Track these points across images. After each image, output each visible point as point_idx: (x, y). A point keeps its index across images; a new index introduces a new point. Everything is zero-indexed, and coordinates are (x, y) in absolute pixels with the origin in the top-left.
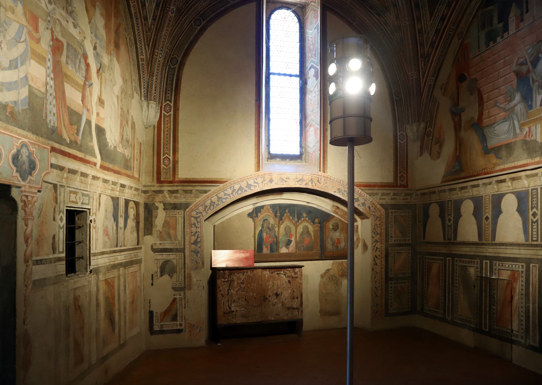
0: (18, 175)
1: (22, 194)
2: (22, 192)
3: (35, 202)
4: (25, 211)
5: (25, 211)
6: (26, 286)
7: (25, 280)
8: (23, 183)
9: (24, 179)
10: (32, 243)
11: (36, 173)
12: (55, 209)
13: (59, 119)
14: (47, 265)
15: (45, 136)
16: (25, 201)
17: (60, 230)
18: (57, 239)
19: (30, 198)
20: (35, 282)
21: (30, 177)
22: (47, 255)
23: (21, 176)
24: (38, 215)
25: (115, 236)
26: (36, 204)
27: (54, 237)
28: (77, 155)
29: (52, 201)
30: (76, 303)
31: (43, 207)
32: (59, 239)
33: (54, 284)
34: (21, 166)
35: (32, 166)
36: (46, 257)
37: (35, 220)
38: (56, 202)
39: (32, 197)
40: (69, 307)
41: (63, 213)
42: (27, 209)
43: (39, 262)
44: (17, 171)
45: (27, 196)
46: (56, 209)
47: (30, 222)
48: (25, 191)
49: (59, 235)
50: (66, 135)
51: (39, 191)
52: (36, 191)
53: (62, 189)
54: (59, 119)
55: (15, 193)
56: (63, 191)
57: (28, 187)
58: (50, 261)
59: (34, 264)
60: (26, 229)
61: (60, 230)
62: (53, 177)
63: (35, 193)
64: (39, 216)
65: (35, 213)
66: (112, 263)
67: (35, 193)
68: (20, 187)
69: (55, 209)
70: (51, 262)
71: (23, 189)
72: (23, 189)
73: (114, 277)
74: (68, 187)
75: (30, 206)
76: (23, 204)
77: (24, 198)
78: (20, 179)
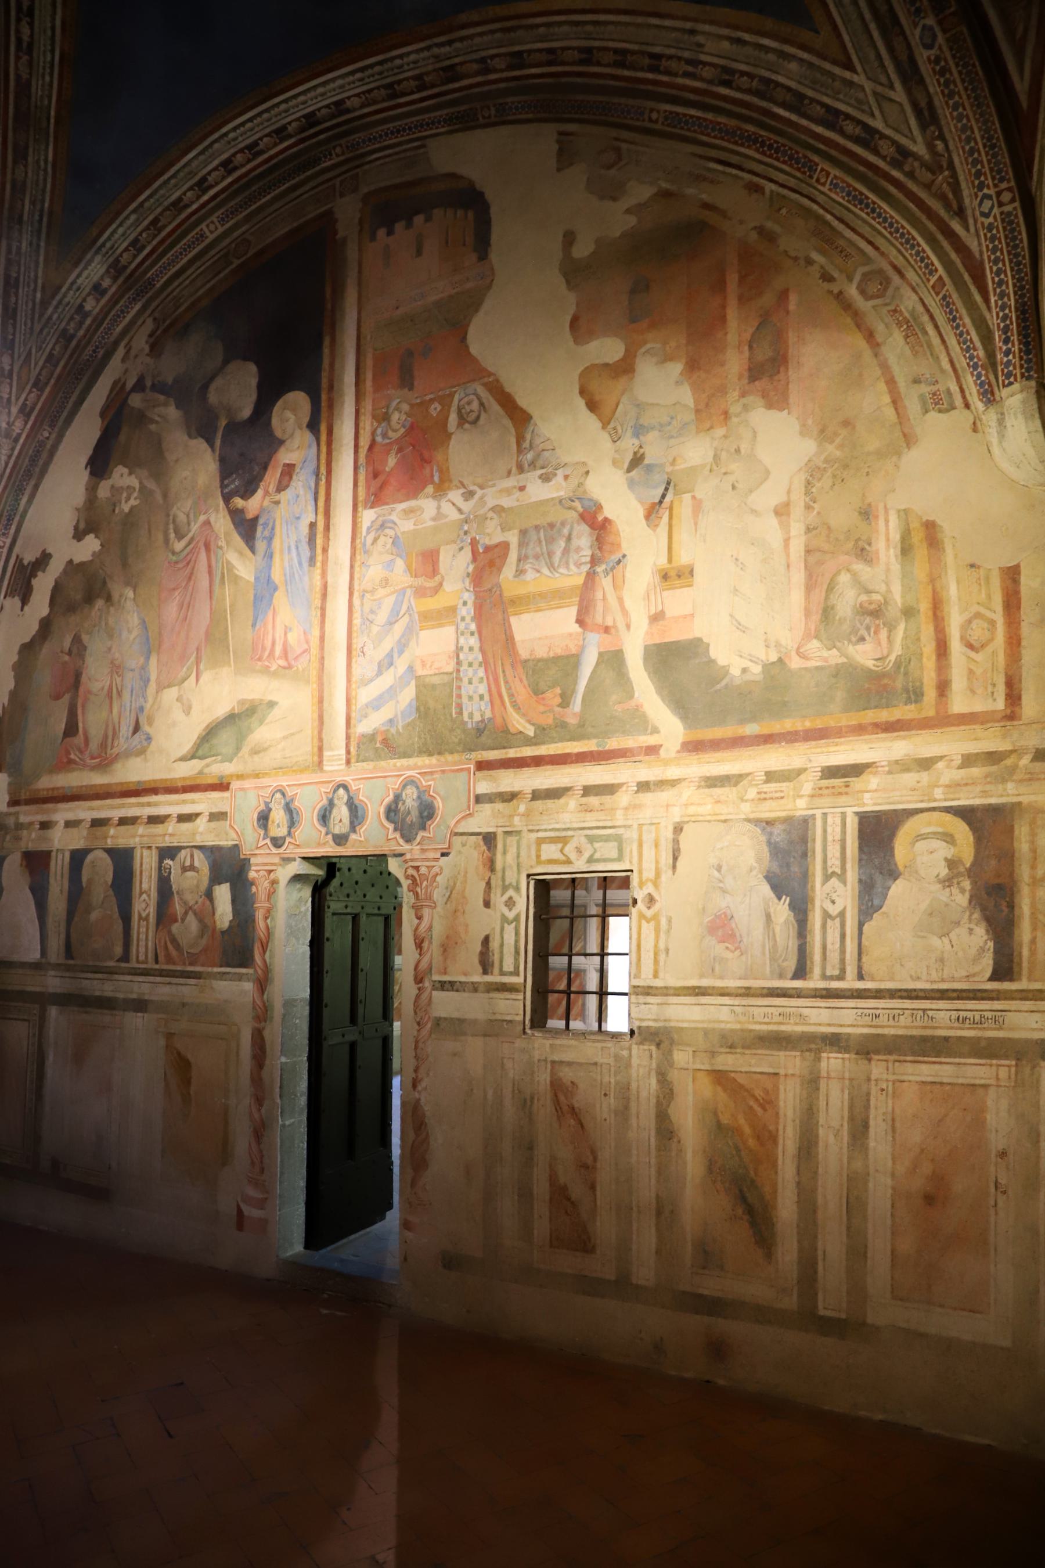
0: (398, 835)
1: (406, 865)
2: (406, 861)
3: (437, 874)
4: (416, 894)
5: (416, 894)
6: (419, 1024)
7: (415, 1012)
8: (407, 847)
9: (408, 840)
10: (434, 950)
11: (432, 825)
12: (488, 884)
13: (497, 701)
14: (466, 995)
15: (460, 749)
16: (412, 876)
17: (506, 925)
18: (494, 944)
19: (423, 870)
20: (438, 1021)
21: (421, 834)
22: (465, 974)
23: (402, 836)
24: (445, 899)
25: (793, 944)
26: (438, 878)
27: (486, 940)
28: (568, 751)
29: (481, 867)
30: (562, 1098)
31: (455, 884)
32: (502, 945)
33: (485, 1035)
34: (403, 820)
35: (427, 812)
36: (463, 979)
37: (439, 909)
38: (492, 869)
39: (428, 867)
40: (532, 1098)
41: (517, 889)
42: (419, 890)
43: (447, 986)
44: (395, 830)
45: (417, 868)
46: (493, 882)
47: (426, 912)
48: (412, 860)
49: (502, 938)
50: (522, 721)
51: (443, 855)
52: (438, 855)
53: (512, 840)
54: (497, 701)
55: (394, 866)
56: (515, 842)
57: (418, 852)
58: (475, 988)
59: (434, 988)
60: (418, 925)
61: (506, 925)
62: (484, 819)
63: (436, 860)
64: (448, 900)
65: (438, 895)
66: (757, 1027)
67: (436, 860)
68: (401, 855)
69: (488, 884)
70: (476, 990)
71: (408, 856)
72: (408, 856)
73: (776, 1074)
74: (530, 831)
75: (425, 884)
76: (410, 882)
77: (411, 871)
78: (401, 841)
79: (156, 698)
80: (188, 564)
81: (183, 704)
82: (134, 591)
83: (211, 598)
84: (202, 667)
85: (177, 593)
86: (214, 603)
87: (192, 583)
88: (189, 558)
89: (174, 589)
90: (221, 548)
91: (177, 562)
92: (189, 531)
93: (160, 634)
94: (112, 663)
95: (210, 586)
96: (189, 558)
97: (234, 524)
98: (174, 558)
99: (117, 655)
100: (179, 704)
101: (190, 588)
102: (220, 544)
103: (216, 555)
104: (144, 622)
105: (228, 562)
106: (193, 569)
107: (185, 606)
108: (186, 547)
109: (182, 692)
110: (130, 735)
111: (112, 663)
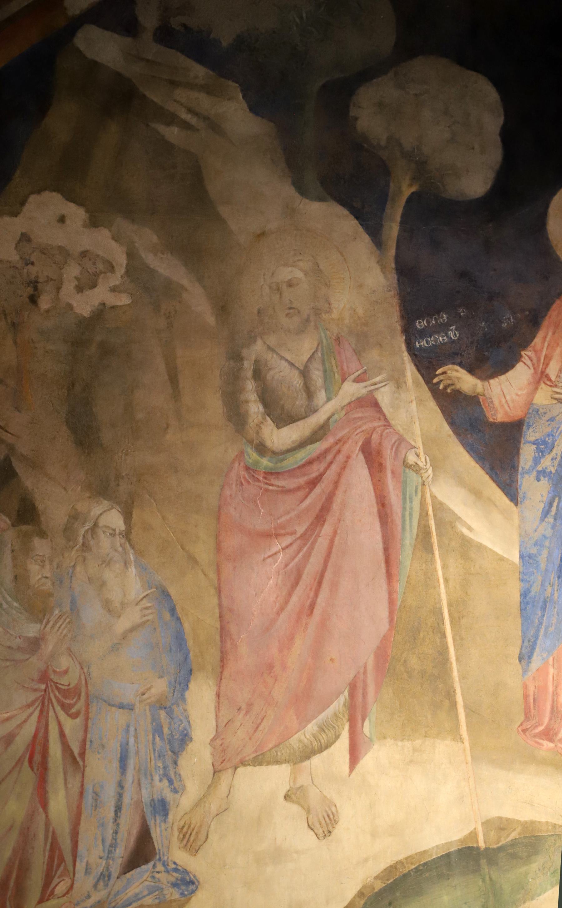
79: (212, 787)
80: (313, 483)
81: (308, 811)
82: (128, 516)
83: (389, 576)
84: (367, 728)
85: (277, 546)
86: (400, 587)
87: (327, 529)
88: (315, 470)
89: (268, 535)
90: (416, 468)
91: (270, 473)
92: (312, 410)
93: (223, 632)
94: (44, 677)
95: (386, 549)
96: (315, 470)
97: (452, 423)
98: (265, 462)
99: (64, 662)
100: (294, 808)
101: (322, 543)
102: (411, 459)
103: (403, 485)
104: (166, 595)
105: (439, 507)
106: (330, 498)
107: (307, 578)
108: (302, 444)
109: (303, 780)
110: (116, 867)
111: (44, 677)
